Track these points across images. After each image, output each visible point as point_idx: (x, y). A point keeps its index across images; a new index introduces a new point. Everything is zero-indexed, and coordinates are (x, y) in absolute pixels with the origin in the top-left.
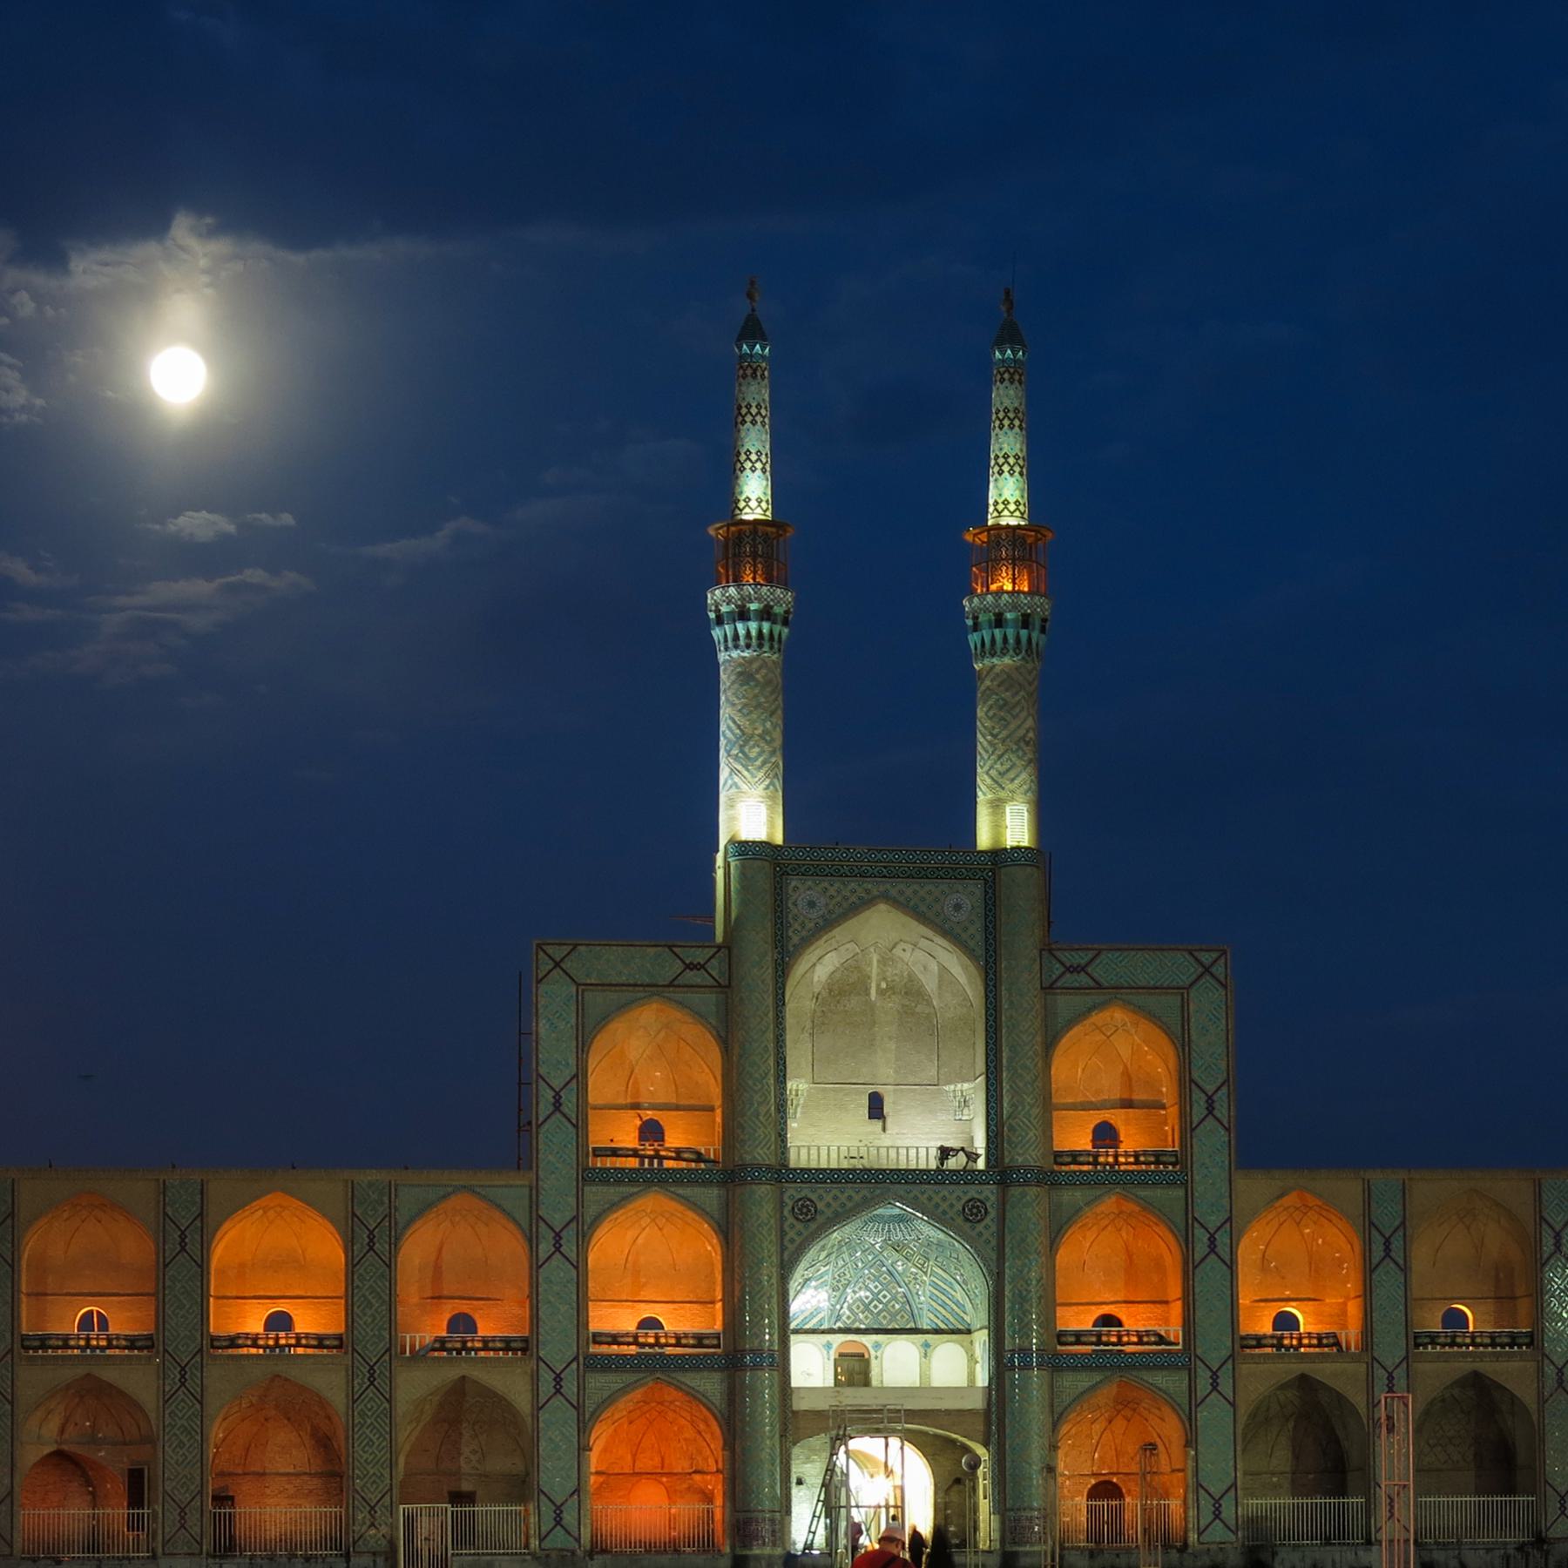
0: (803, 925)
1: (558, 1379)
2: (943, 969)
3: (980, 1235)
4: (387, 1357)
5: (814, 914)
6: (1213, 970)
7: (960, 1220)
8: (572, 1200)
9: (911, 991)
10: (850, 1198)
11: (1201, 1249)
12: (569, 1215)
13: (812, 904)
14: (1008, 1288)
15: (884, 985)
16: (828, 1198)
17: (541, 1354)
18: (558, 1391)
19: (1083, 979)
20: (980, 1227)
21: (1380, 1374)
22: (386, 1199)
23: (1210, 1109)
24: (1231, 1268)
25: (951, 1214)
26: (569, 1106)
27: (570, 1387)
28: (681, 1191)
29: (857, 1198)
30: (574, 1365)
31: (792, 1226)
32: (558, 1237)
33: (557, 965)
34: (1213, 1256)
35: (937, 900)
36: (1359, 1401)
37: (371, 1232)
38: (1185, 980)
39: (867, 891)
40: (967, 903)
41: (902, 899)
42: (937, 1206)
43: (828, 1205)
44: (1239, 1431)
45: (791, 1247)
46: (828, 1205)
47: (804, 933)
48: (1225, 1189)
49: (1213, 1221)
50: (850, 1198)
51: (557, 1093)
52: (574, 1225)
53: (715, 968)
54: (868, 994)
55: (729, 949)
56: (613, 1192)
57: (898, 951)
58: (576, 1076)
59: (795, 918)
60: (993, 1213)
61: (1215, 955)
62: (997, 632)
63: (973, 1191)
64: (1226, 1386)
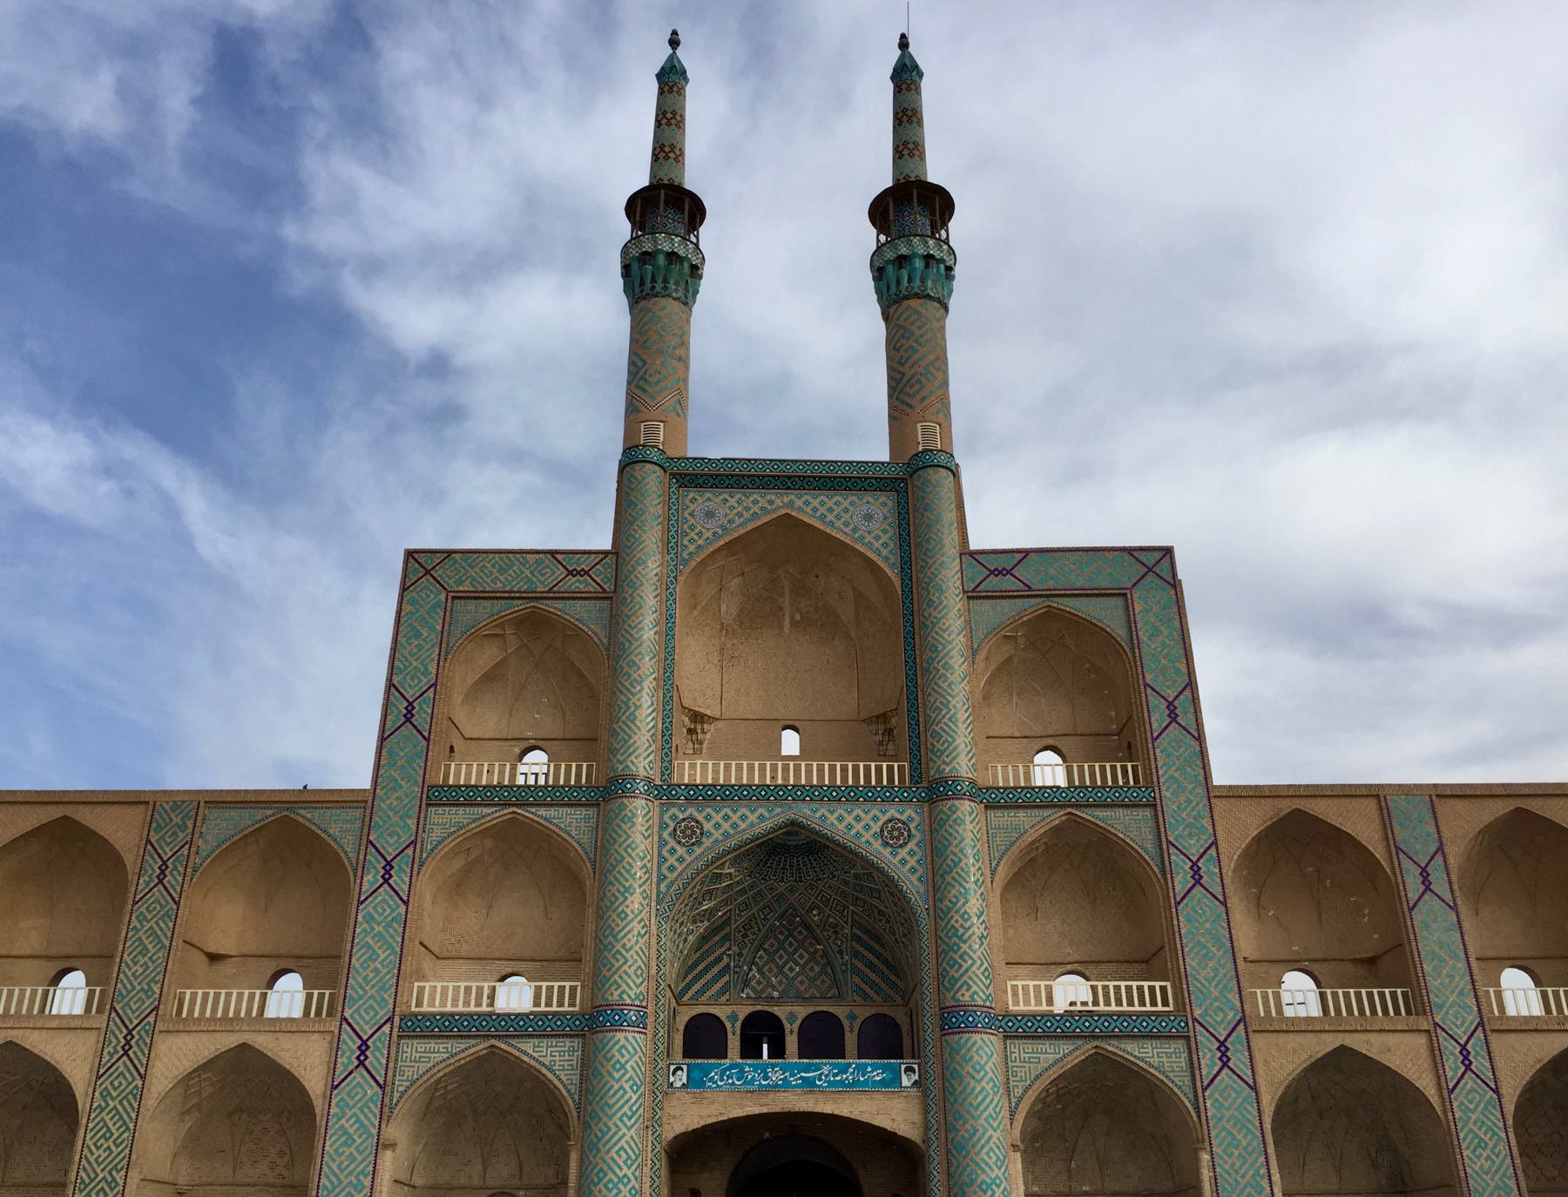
0: (700, 534)
1: (364, 1047)
3: (903, 862)
4: (151, 1019)
5: (713, 524)
6: (1157, 569)
7: (877, 844)
8: (412, 823)
10: (744, 818)
11: (1182, 880)
12: (406, 838)
13: (710, 514)
15: (798, 617)
16: (718, 818)
17: (346, 1015)
18: (361, 1063)
19: (1008, 583)
20: (903, 853)
21: (1451, 1048)
22: (190, 824)
23: (1173, 716)
24: (1224, 903)
25: (867, 836)
26: (421, 718)
27: (376, 1059)
29: (752, 818)
30: (386, 1029)
31: (672, 851)
32: (389, 865)
33: (428, 572)
34: (1198, 888)
35: (846, 511)
36: (1425, 1083)
37: (164, 863)
38: (1126, 582)
39: (771, 502)
40: (879, 514)
41: (808, 509)
43: (717, 826)
44: (1268, 1126)
45: (671, 876)
46: (717, 826)
48: (1203, 806)
49: (1194, 846)
50: (744, 818)
51: (410, 704)
52: (410, 851)
53: (603, 575)
54: (781, 627)
55: (617, 554)
56: (461, 815)
58: (434, 685)
59: (692, 528)
60: (917, 836)
61: (1158, 555)
62: (905, 274)
63: (892, 812)
64: (1239, 1060)
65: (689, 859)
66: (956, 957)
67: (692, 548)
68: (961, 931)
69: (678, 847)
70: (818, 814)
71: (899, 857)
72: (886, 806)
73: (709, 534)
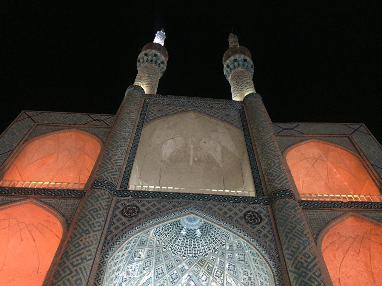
2: (223, 148)
3: (259, 231)
7: (243, 222)
9: (210, 161)
13: (160, 110)
14: (289, 263)
15: (196, 159)
16: (149, 205)
20: (258, 227)
28: (48, 201)
33: (30, 117)
42: (226, 213)
43: (148, 209)
45: (115, 232)
47: (156, 117)
54: (188, 161)
57: (202, 144)
60: (266, 220)
62: (236, 63)
63: (250, 207)
65: (128, 223)
66: (306, 280)
67: (151, 118)
68: (306, 264)
69: (123, 218)
70: (207, 207)
71: (256, 229)
72: (246, 205)
73: (160, 115)
